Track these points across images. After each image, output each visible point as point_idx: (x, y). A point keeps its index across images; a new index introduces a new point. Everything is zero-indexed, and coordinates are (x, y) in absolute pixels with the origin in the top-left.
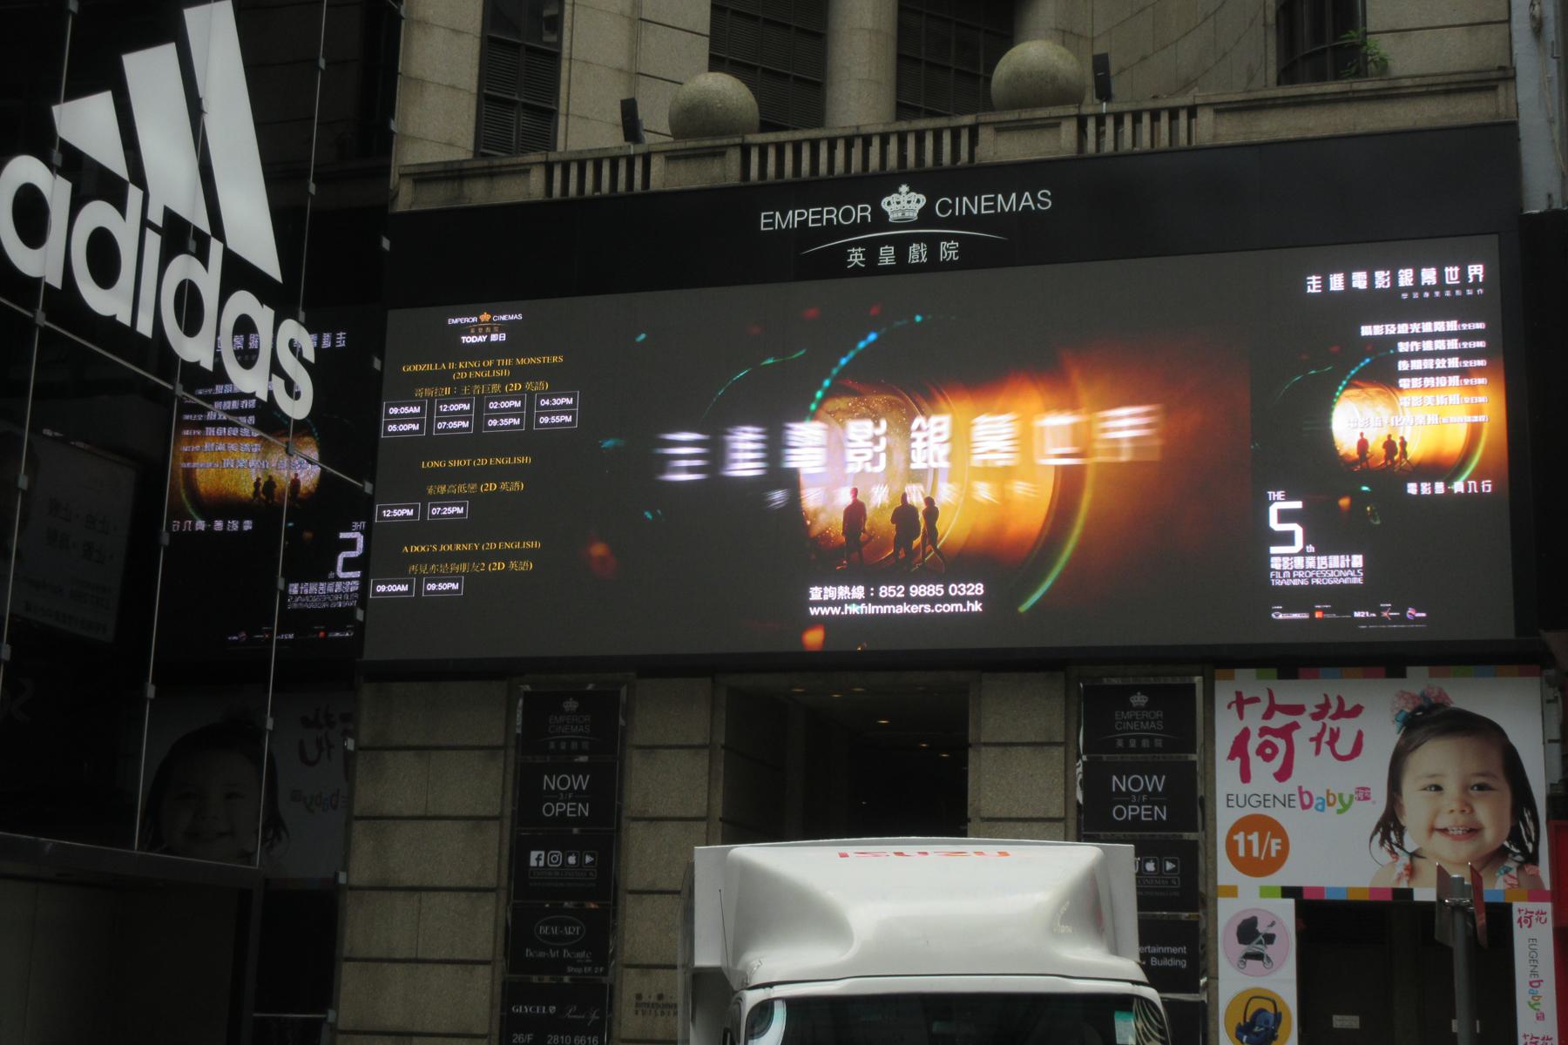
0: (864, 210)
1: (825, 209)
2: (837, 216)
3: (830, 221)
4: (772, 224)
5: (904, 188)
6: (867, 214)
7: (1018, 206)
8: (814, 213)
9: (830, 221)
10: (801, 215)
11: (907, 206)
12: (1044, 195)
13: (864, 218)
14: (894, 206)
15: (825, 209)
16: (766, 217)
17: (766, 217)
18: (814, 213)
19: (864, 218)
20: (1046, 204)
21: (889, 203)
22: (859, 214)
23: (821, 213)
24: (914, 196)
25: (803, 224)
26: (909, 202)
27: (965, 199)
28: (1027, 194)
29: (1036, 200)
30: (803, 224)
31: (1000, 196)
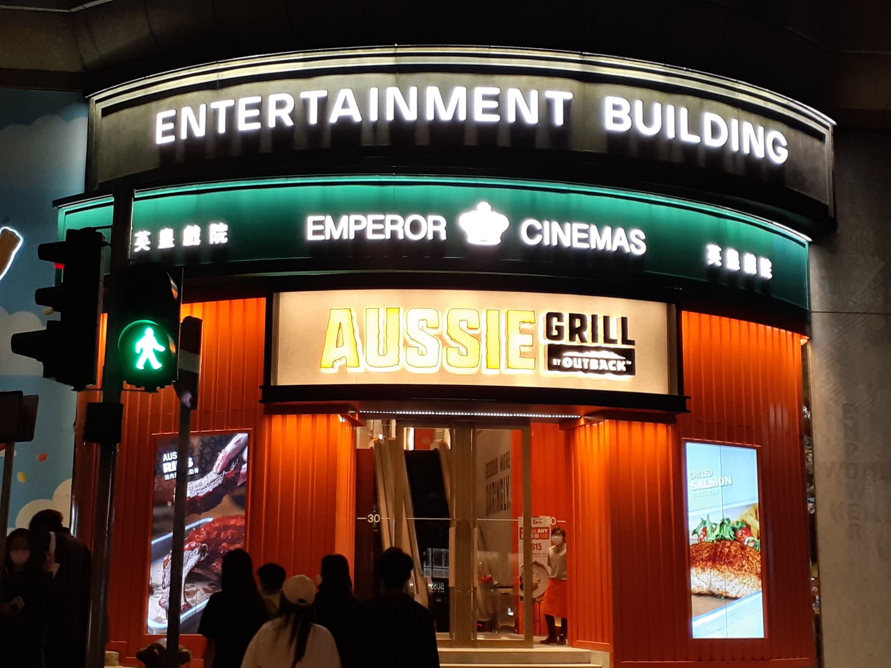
3: (394, 233)
4: (320, 232)
9: (394, 233)
10: (357, 222)
13: (436, 234)
16: (315, 223)
17: (315, 223)
18: (375, 222)
19: (436, 234)
25: (360, 235)
30: (360, 235)
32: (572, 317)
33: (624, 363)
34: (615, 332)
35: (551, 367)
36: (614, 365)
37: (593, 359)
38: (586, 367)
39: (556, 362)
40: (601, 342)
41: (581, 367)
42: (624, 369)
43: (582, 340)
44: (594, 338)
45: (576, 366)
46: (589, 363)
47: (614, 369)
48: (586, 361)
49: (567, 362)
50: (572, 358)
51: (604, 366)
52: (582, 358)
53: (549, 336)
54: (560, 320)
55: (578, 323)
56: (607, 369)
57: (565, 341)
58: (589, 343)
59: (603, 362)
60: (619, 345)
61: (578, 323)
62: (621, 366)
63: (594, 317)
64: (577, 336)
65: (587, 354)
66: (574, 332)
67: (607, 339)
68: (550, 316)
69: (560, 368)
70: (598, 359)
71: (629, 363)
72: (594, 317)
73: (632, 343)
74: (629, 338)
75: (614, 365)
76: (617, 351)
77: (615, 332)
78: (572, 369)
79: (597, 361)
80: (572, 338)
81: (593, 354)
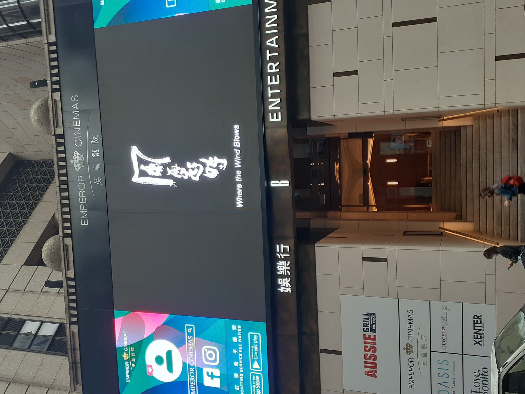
34: (366, 317)
41: (374, 326)
43: (368, 324)
44: (368, 322)
48: (373, 324)
49: (374, 328)
50: (373, 327)
52: (373, 325)
53: (368, 331)
55: (365, 325)
57: (369, 328)
58: (369, 323)
59: (373, 320)
60: (369, 316)
61: (365, 325)
62: (374, 316)
63: (363, 321)
64: (368, 325)
67: (368, 319)
68: (364, 331)
69: (375, 330)
70: (372, 321)
72: (363, 321)
73: (368, 313)
77: (366, 317)
78: (375, 327)
80: (368, 326)
81: (371, 322)
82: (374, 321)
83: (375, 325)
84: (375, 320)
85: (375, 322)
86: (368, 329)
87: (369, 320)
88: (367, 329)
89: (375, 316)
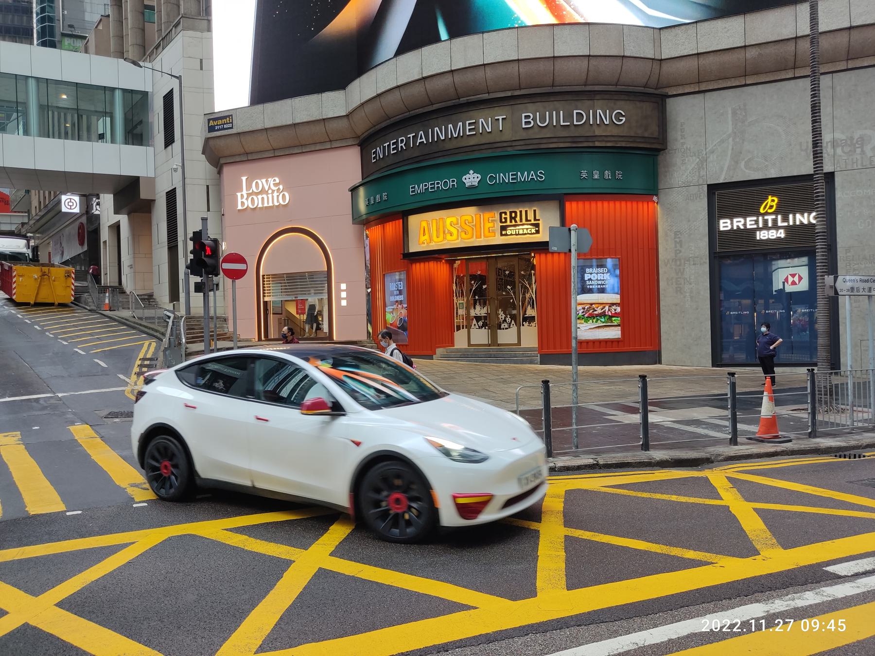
0: (453, 181)
1: (436, 182)
2: (441, 185)
5: (471, 172)
6: (455, 183)
7: (528, 179)
8: (431, 184)
11: (473, 180)
12: (540, 173)
14: (468, 180)
15: (436, 182)
20: (541, 177)
21: (465, 179)
22: (451, 184)
23: (434, 184)
24: (476, 175)
26: (474, 178)
27: (501, 174)
28: (532, 172)
29: (537, 176)
31: (519, 173)
32: (511, 213)
33: (535, 229)
35: (502, 235)
36: (530, 231)
37: (521, 229)
38: (517, 233)
39: (504, 232)
40: (524, 221)
42: (535, 232)
43: (516, 221)
44: (521, 220)
45: (513, 233)
46: (519, 231)
47: (530, 232)
48: (517, 231)
49: (509, 232)
50: (511, 230)
51: (525, 231)
53: (501, 222)
54: (506, 213)
55: (513, 215)
56: (527, 233)
57: (508, 223)
58: (519, 223)
59: (525, 230)
60: (533, 222)
61: (513, 215)
62: (533, 231)
64: (513, 220)
65: (518, 228)
66: (511, 218)
67: (527, 220)
69: (506, 235)
70: (523, 229)
71: (537, 229)
73: (539, 220)
74: (537, 218)
75: (530, 231)
76: (532, 224)
77: (531, 216)
78: (511, 235)
79: (522, 230)
80: (511, 222)
82: (523, 231)
83: (516, 235)
84: (525, 234)
85: (521, 234)
86: (506, 222)
87: (524, 221)
88: (506, 219)
89: (534, 234)
